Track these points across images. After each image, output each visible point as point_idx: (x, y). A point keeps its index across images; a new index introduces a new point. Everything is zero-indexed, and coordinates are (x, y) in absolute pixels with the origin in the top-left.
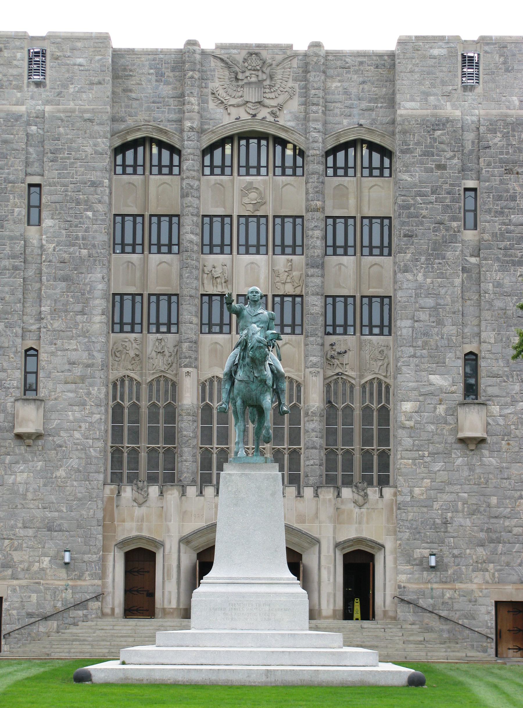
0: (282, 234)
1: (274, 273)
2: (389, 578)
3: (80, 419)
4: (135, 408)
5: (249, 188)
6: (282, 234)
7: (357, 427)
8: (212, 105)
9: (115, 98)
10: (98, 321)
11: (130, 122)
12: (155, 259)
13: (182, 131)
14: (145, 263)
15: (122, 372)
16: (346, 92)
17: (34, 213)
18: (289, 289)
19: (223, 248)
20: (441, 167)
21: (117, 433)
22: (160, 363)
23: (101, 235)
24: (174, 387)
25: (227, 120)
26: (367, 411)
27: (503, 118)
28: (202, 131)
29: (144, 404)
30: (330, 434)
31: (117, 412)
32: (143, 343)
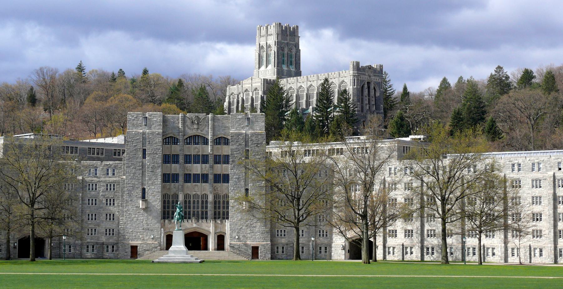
0: (205, 159)
1: (202, 168)
2: (227, 242)
3: (156, 203)
4: (169, 201)
5: (196, 148)
6: (205, 159)
7: (221, 205)
8: (187, 129)
9: (163, 127)
10: (159, 180)
11: (167, 133)
12: (173, 165)
13: (179, 135)
14: (171, 166)
15: (165, 192)
16: (219, 126)
17: (144, 157)
18: (205, 172)
19: (190, 163)
20: (240, 145)
21: (164, 207)
22: (175, 190)
23: (160, 161)
24: (177, 196)
25: (190, 132)
26: (224, 202)
27: (255, 133)
28: (184, 135)
29: (171, 200)
30: (215, 207)
31: (164, 202)
32: (170, 185)
